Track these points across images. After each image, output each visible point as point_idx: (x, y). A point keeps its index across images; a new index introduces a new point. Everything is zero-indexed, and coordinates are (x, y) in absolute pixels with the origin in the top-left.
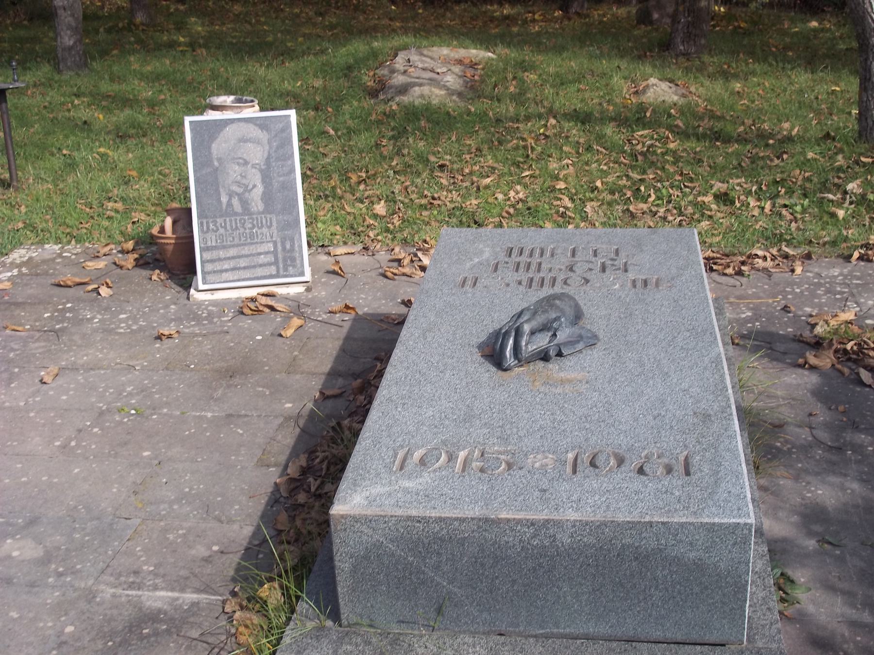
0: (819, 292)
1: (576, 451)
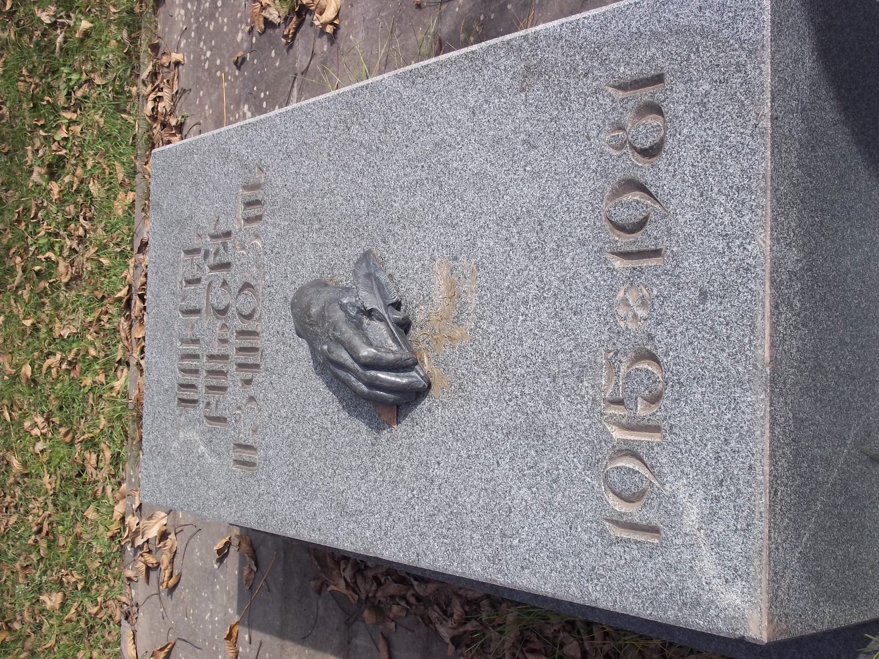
0: (211, 28)
1: (609, 256)
